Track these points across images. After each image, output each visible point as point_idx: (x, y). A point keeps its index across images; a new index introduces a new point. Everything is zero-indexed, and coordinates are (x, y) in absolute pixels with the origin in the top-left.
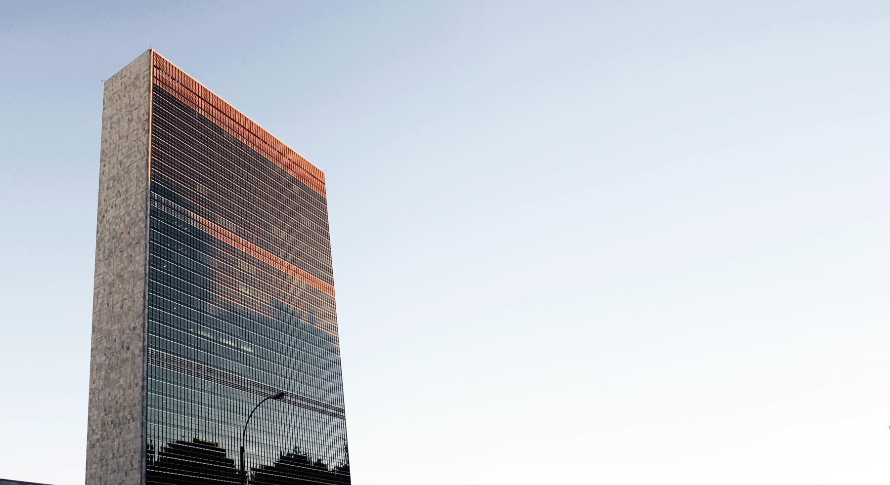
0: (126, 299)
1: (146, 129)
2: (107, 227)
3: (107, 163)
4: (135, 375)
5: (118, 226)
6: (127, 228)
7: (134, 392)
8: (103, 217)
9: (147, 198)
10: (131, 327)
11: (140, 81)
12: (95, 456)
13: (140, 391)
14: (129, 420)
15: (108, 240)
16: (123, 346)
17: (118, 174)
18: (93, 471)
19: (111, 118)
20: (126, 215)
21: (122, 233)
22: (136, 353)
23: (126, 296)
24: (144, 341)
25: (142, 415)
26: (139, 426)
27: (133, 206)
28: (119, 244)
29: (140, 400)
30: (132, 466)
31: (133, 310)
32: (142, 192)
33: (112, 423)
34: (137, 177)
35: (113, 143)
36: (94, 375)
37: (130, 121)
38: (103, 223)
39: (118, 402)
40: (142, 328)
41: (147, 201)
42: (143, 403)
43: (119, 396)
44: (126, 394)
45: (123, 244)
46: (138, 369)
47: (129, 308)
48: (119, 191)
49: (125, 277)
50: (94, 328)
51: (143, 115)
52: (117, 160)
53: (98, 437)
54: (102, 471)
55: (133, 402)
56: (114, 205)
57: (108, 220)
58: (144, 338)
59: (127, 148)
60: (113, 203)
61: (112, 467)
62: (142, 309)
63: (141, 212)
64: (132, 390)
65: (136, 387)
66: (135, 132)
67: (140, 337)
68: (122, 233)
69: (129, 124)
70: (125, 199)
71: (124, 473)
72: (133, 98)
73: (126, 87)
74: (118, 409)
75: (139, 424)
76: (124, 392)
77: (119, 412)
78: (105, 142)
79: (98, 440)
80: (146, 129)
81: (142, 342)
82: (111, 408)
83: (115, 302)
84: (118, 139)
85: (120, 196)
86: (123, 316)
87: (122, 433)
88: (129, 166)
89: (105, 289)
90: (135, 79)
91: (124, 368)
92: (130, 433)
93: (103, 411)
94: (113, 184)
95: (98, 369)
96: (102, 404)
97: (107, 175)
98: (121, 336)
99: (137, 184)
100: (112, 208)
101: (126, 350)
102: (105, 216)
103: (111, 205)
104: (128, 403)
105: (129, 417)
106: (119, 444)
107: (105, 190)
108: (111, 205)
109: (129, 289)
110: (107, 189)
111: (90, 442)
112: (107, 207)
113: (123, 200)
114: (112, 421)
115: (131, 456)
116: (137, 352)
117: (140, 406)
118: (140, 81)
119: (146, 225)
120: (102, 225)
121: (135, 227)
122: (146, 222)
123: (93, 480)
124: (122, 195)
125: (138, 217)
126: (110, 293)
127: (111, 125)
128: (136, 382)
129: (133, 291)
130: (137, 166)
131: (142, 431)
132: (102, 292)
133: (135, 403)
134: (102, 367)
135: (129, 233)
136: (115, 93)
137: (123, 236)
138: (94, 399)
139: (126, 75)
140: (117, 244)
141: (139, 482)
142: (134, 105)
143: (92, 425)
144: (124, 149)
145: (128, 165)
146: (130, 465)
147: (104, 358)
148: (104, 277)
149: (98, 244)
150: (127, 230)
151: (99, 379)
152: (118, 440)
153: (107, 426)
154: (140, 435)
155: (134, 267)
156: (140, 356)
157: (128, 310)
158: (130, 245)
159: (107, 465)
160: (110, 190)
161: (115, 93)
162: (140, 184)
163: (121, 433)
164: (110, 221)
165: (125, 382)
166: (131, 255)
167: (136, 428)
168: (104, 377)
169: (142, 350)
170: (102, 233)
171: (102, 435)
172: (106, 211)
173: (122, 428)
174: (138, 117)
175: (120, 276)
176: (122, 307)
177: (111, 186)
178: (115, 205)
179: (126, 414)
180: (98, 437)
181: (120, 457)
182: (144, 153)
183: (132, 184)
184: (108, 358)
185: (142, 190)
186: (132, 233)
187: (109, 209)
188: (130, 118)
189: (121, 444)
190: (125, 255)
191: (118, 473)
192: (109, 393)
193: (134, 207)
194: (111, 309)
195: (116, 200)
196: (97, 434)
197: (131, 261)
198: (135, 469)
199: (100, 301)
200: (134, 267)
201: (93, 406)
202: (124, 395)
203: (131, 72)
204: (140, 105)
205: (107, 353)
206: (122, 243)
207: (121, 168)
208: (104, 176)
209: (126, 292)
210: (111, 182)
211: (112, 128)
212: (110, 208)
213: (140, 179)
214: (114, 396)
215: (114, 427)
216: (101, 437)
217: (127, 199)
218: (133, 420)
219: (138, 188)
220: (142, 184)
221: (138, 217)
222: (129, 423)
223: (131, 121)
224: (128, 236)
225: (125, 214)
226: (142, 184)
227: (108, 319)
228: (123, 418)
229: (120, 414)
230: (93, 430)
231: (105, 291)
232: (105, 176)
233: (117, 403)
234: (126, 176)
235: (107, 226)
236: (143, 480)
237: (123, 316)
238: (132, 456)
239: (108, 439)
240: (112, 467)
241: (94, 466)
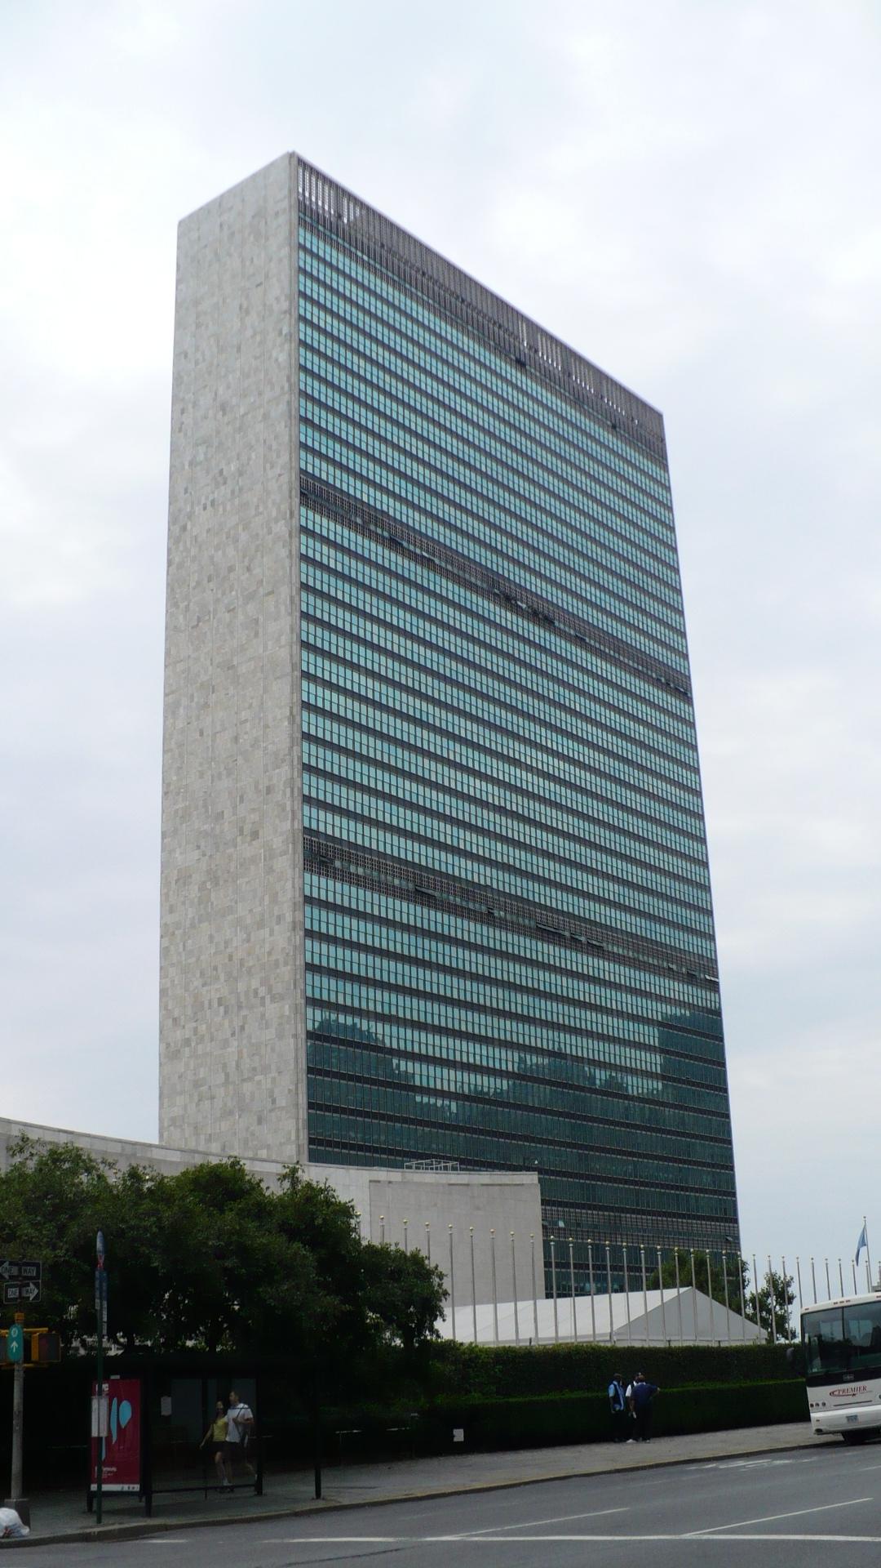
0: (246, 721)
1: (285, 330)
2: (192, 553)
3: (190, 406)
4: (274, 900)
5: (220, 552)
6: (244, 557)
7: (271, 934)
8: (184, 528)
9: (291, 492)
10: (261, 787)
11: (266, 223)
12: (180, 1077)
13: (289, 934)
14: (263, 998)
15: (198, 583)
17: (218, 432)
18: (177, 1111)
19: (197, 303)
20: (240, 528)
21: (231, 569)
22: (274, 847)
23: (244, 715)
24: (293, 820)
25: (295, 987)
26: (287, 1013)
27: (257, 507)
28: (224, 594)
29: (287, 954)
30: (274, 1101)
31: (266, 748)
32: (280, 475)
33: (220, 1004)
34: (265, 441)
35: (204, 360)
36: (171, 893)
37: (244, 311)
38: (181, 545)
39: (235, 958)
40: (288, 790)
41: (291, 497)
42: (295, 960)
43: (235, 945)
44: (252, 939)
45: (234, 593)
46: (282, 883)
47: (255, 744)
48: (221, 472)
49: (243, 669)
50: (166, 784)
51: (277, 299)
52: (215, 400)
53: (188, 1033)
54: (199, 1111)
55: (273, 958)
56: (209, 503)
58: (293, 812)
59: (238, 373)
60: (207, 498)
61: (225, 1105)
62: (288, 745)
63: (276, 521)
64: (267, 930)
65: (278, 923)
66: (258, 338)
67: (284, 810)
68: (231, 569)
69: (242, 320)
71: (255, 1118)
72: (252, 259)
73: (233, 234)
74: (235, 974)
75: (287, 1007)
76: (249, 935)
77: (236, 980)
78: (183, 356)
79: (187, 1042)
80: (284, 332)
81: (289, 822)
82: (215, 969)
83: (218, 728)
84: (215, 350)
85: (225, 483)
86: (240, 761)
87: (246, 1026)
88: (246, 414)
89: (192, 696)
90: (253, 217)
91: (247, 880)
92: (267, 1028)
93: (198, 975)
94: (205, 454)
95: (181, 881)
96: (194, 960)
97: (189, 434)
98: (235, 807)
99: (265, 456)
100: (205, 508)
101: (249, 838)
102: (189, 527)
103: (203, 501)
104: (259, 960)
105: (262, 991)
106: (240, 1052)
107: (187, 467)
108: (203, 501)
109: (252, 698)
110: (191, 464)
111: (168, 1045)
112: (192, 507)
113: (233, 492)
114: (220, 999)
115: (269, 1081)
116: (278, 843)
117: (289, 967)
118: (266, 223)
119: (290, 551)
120: (181, 548)
121: (262, 557)
122: (291, 545)
123: (179, 1130)
124: (229, 482)
125: (270, 533)
126: (206, 705)
127: (197, 318)
128: (276, 913)
129: (262, 704)
130: (264, 414)
131: (296, 1023)
132: (184, 701)
133: (277, 964)
134: (190, 876)
135: (249, 569)
136: (206, 246)
137: (232, 576)
138: (172, 948)
139: (232, 208)
140: (220, 592)
141: (293, 1137)
142: (254, 275)
143: (170, 1008)
144: (231, 376)
145: (242, 411)
146: (270, 1100)
147: (196, 854)
148: (189, 668)
149: (172, 590)
150: (243, 562)
151: (184, 903)
152: (236, 1043)
153: (208, 1012)
154: (294, 1032)
155: (265, 648)
156: (285, 853)
157: (252, 746)
158: (250, 597)
159: (212, 1098)
160: (198, 468)
161: (206, 246)
162: (275, 456)
163: (242, 1028)
164: (199, 539)
165: (251, 911)
166: (257, 621)
167: (282, 1017)
168: (196, 900)
169: (291, 840)
170: (180, 566)
171: (195, 1030)
172: (190, 516)
173: (245, 1017)
174: (265, 305)
175: (229, 669)
176: (236, 739)
177: (201, 457)
179: (255, 983)
180: (188, 1033)
181: (244, 1080)
182: (282, 388)
183: (253, 456)
184: (204, 855)
185: (278, 470)
186: (257, 571)
187: (197, 509)
188: (245, 306)
189: (245, 1050)
190: (241, 617)
191: (240, 1117)
192: (211, 937)
193: (261, 509)
194: (210, 743)
195: (213, 493)
196: (184, 1027)
197: (256, 635)
198: (281, 1108)
199: (180, 724)
200: (265, 648)
201: (172, 965)
202: (248, 941)
203: (243, 201)
204: (267, 276)
205: (203, 844)
207: (226, 419)
208: (182, 434)
209: (247, 705)
210: (201, 450)
211: (198, 326)
212: (198, 509)
213: (274, 447)
214: (223, 944)
215: (226, 1012)
216: (195, 1034)
217: (241, 490)
218: (273, 999)
219: (268, 466)
220: (278, 456)
221: (270, 533)
222: (263, 1004)
223: (247, 312)
224: (247, 575)
225: (237, 524)
226: (278, 456)
227: (201, 764)
228: (247, 993)
229: (240, 985)
230: (175, 1020)
231: (192, 701)
232: (186, 435)
233: (231, 958)
234: (237, 436)
235: (193, 552)
236: (301, 1134)
237: (240, 761)
238: (274, 1079)
239: (212, 1040)
240: (225, 1105)
241: (180, 1100)
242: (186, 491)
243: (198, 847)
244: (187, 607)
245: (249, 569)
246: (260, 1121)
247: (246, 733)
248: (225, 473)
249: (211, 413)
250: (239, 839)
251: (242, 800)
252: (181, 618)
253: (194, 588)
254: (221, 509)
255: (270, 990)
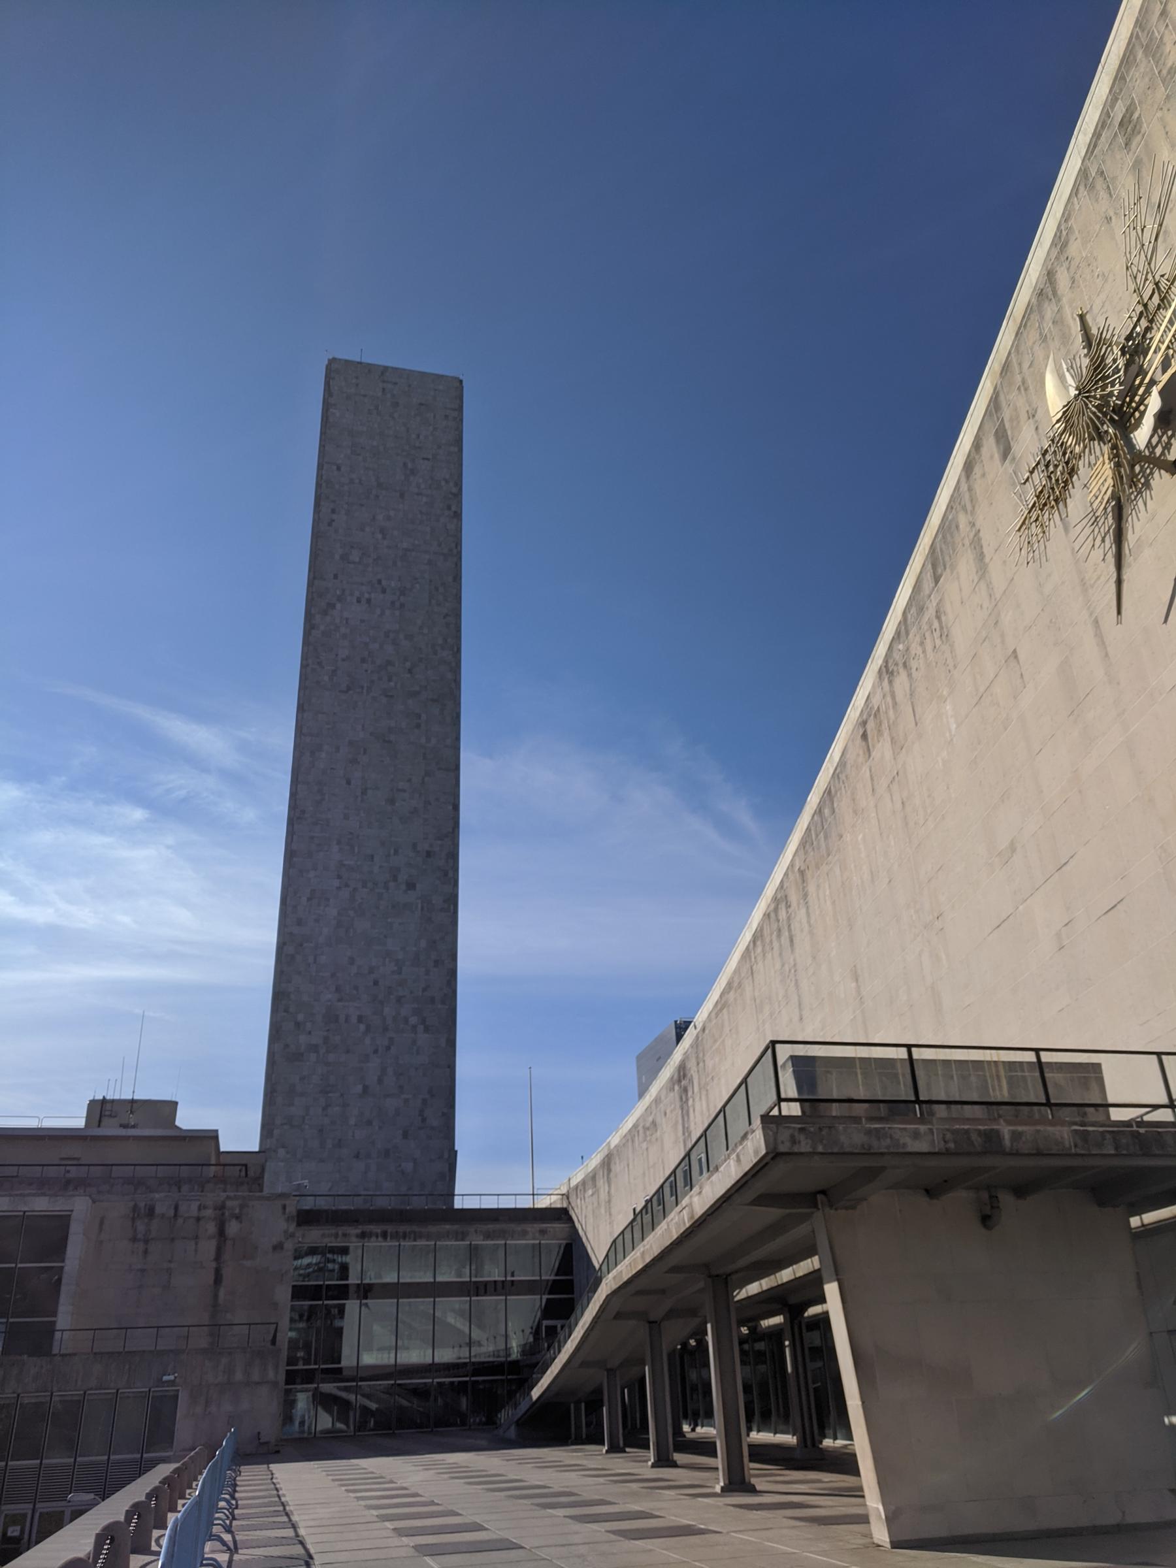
0: (404, 791)
14: (414, 1027)
16: (395, 878)
20: (401, 636)
34: (431, 581)
45: (392, 684)
48: (379, 582)
57: (347, 619)
70: (397, 604)
101: (403, 887)
102: (338, 606)
107: (337, 557)
108: (357, 594)
113: (393, 603)
145: (405, 545)
166: (419, 716)
172: (340, 599)
176: (392, 801)
177: (357, 560)
178: (369, 601)
184: (347, 885)
188: (410, 465)
193: (425, 631)
197: (418, 726)
202: (400, 973)
206: (390, 680)
217: (402, 606)
223: (413, 472)
224: (409, 675)
233: (376, 983)
235: (343, 630)
242: (336, 577)
243: (339, 877)
244: (334, 671)
245: (410, 671)
246: (405, 1135)
247: (404, 800)
248: (384, 583)
249: (367, 529)
250: (392, 884)
251: (396, 852)
252: (326, 678)
253: (343, 660)
254: (378, 611)
255: (423, 1021)
